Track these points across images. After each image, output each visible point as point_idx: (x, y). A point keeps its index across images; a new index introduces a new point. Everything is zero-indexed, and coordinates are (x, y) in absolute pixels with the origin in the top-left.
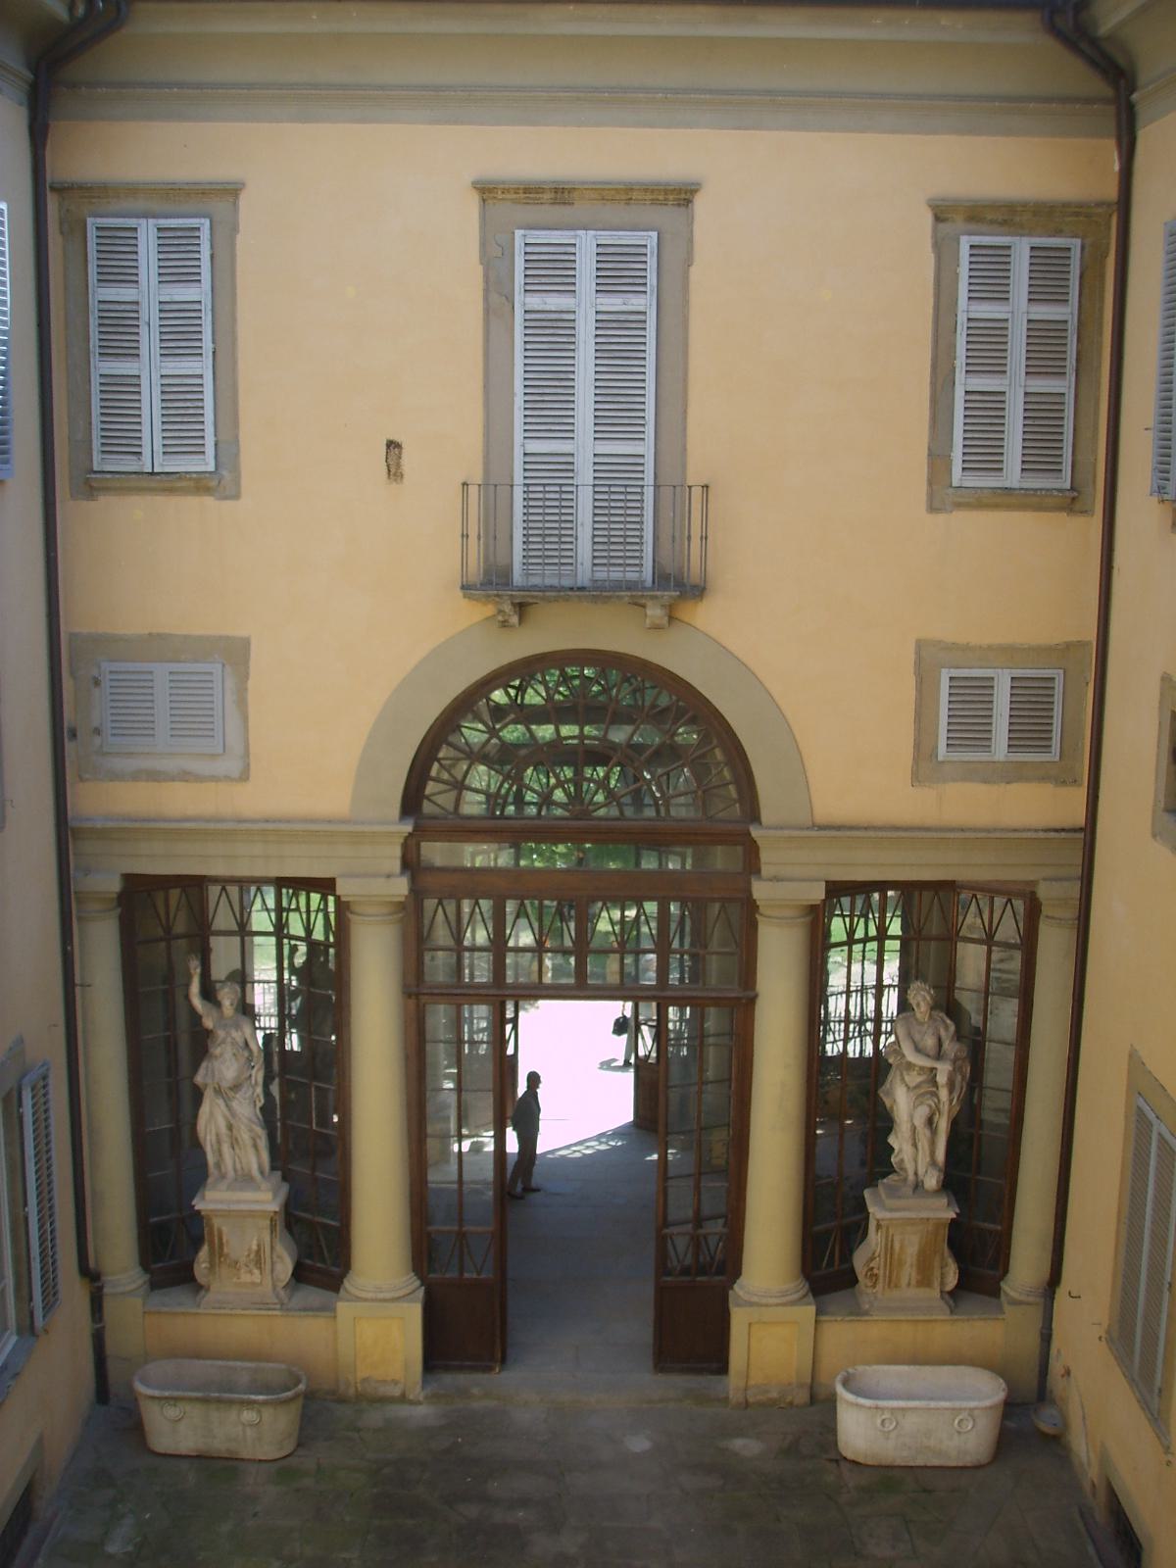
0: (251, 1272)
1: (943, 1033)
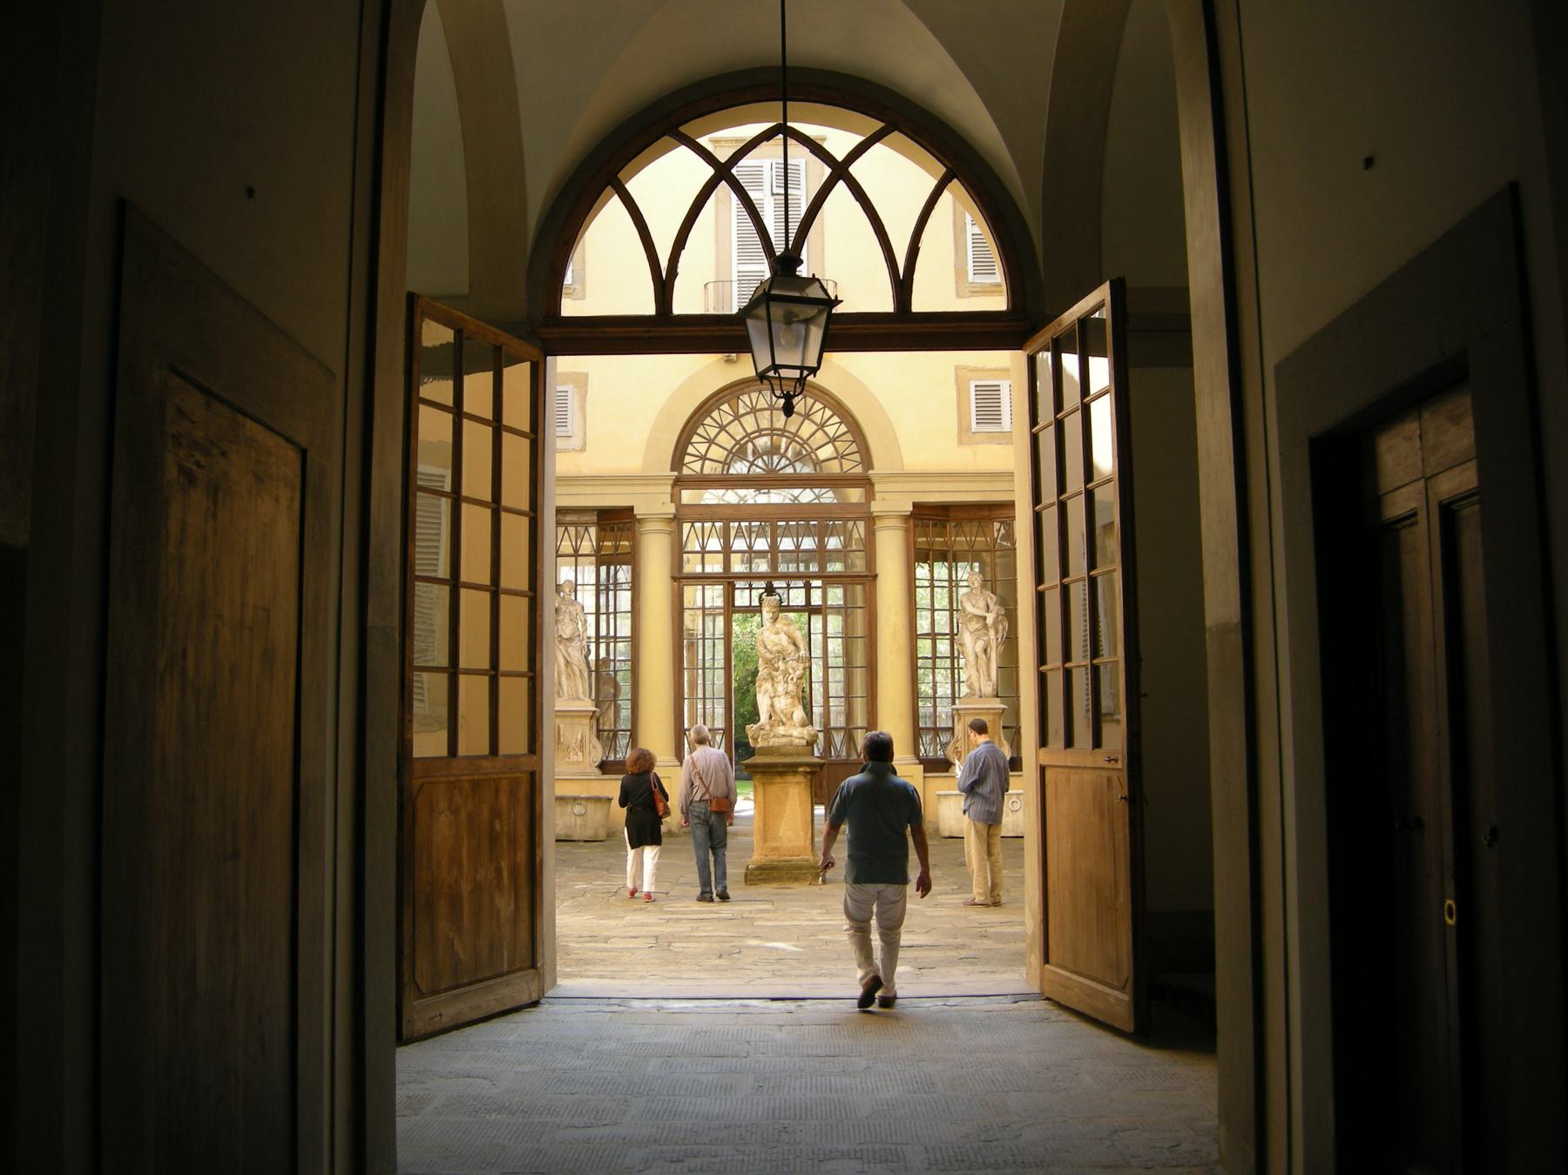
0: (577, 754)
1: (989, 601)
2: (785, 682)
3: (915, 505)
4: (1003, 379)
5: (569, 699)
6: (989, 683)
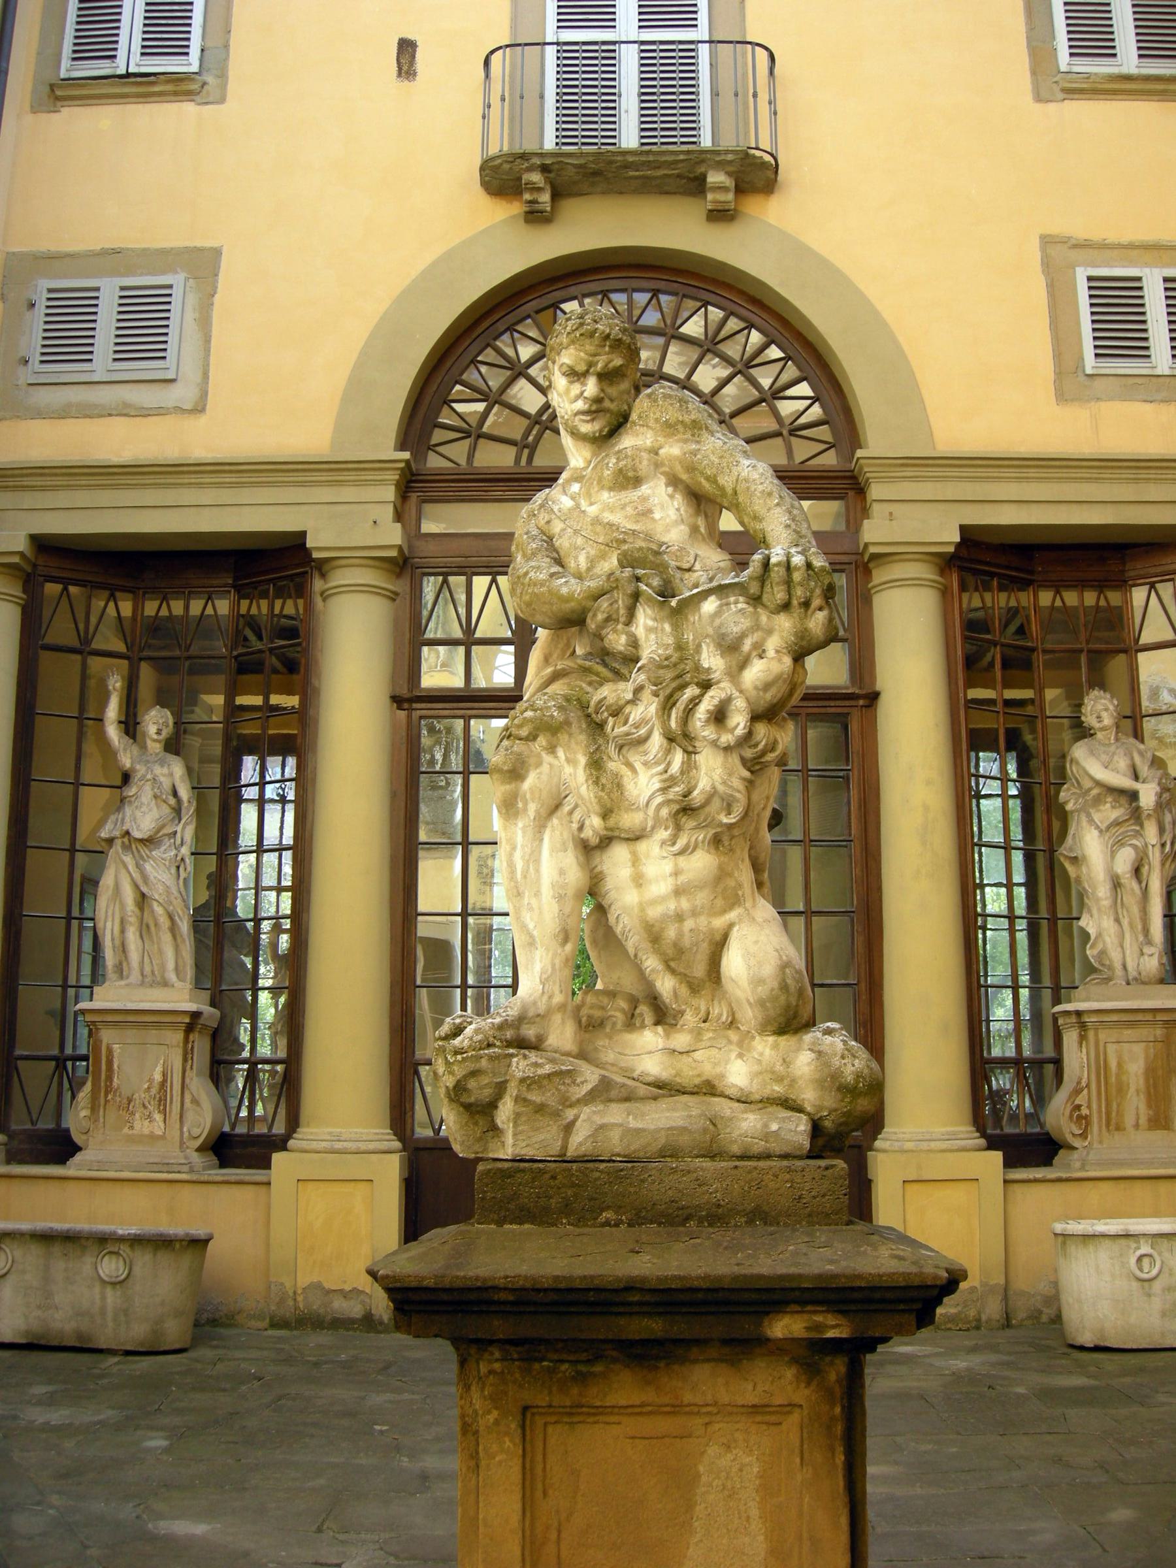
2: (671, 739)
3: (963, 529)
4: (1147, 265)
5: (142, 984)
6: (1152, 950)
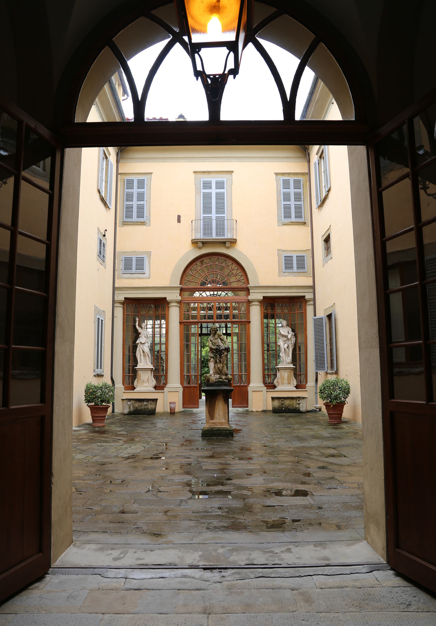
1: (289, 331)
3: (264, 297)
